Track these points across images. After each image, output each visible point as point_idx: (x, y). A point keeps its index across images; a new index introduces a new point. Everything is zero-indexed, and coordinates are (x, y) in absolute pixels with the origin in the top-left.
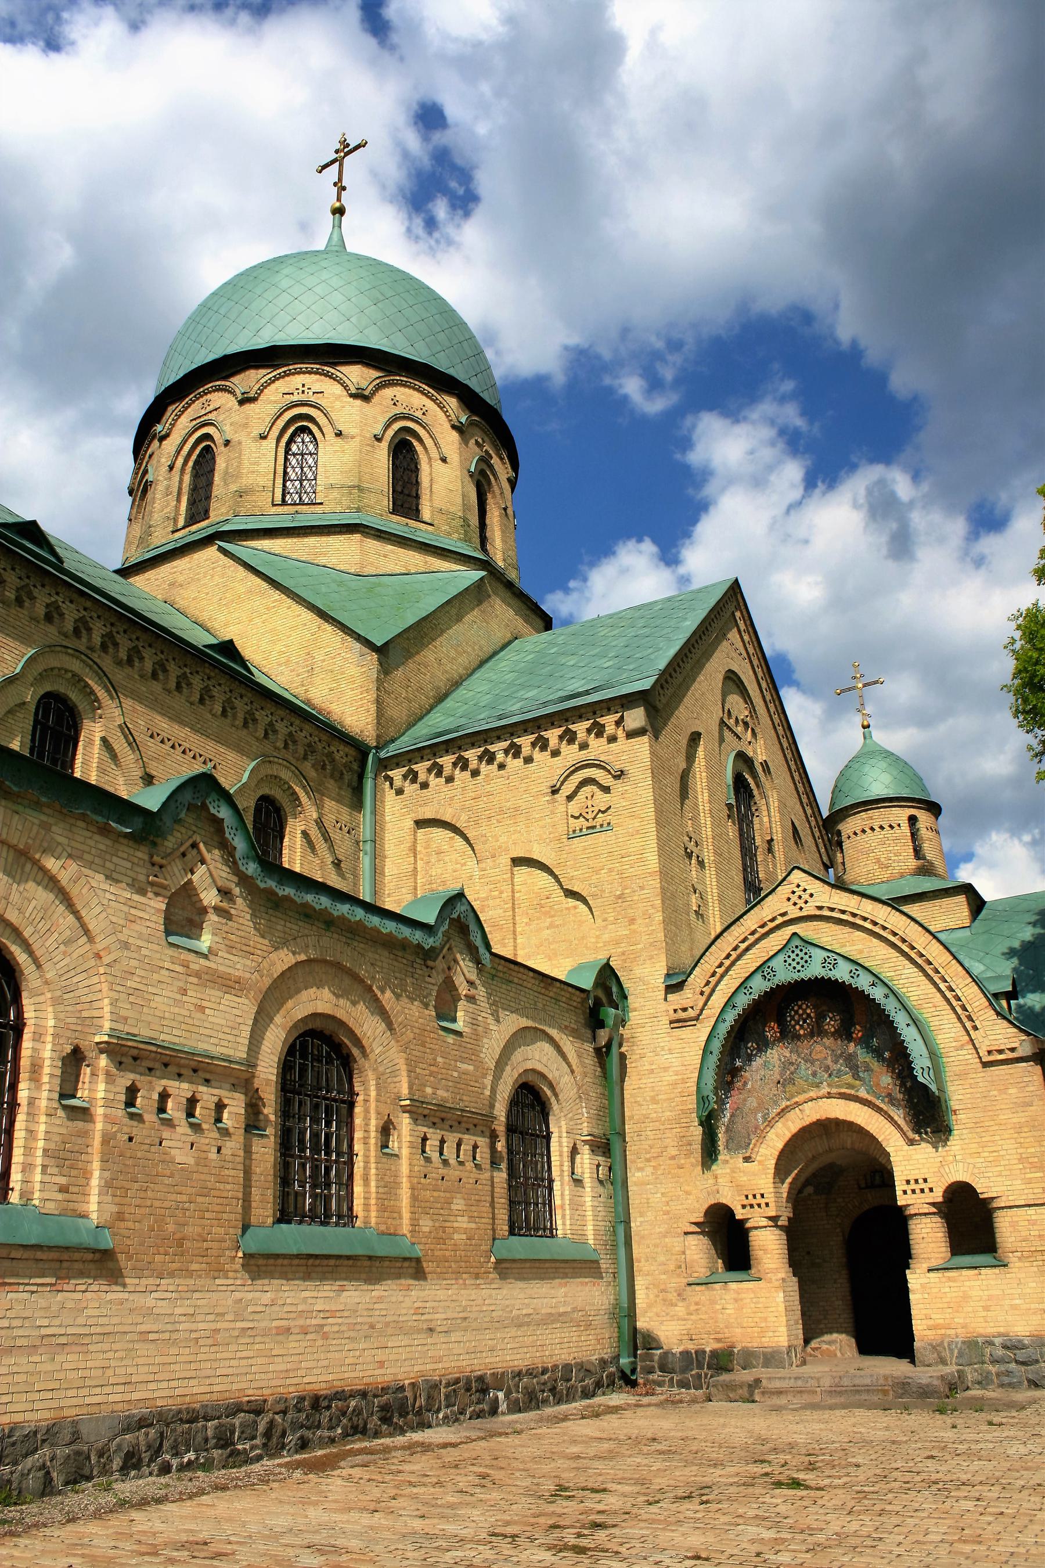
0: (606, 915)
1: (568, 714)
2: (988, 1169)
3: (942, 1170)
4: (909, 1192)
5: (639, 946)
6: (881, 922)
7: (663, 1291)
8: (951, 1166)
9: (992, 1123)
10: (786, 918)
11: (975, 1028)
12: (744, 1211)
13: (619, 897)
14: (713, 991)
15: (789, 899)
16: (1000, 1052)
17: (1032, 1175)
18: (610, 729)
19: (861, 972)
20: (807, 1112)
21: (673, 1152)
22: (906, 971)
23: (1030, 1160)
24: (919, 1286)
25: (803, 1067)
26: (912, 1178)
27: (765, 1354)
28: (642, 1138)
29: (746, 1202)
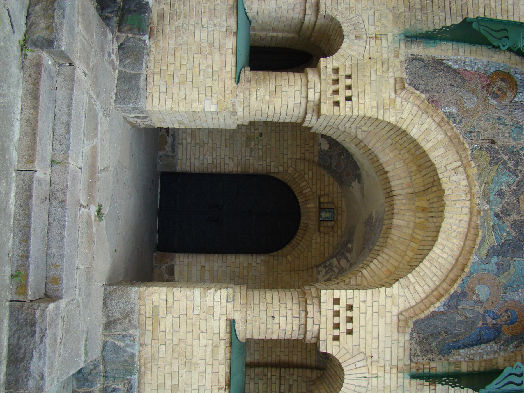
3: (361, 356)
4: (336, 308)
8: (364, 370)
12: (330, 70)
20: (454, 178)
24: (210, 304)
25: (511, 180)
26: (355, 314)
27: (137, 76)
29: (342, 73)
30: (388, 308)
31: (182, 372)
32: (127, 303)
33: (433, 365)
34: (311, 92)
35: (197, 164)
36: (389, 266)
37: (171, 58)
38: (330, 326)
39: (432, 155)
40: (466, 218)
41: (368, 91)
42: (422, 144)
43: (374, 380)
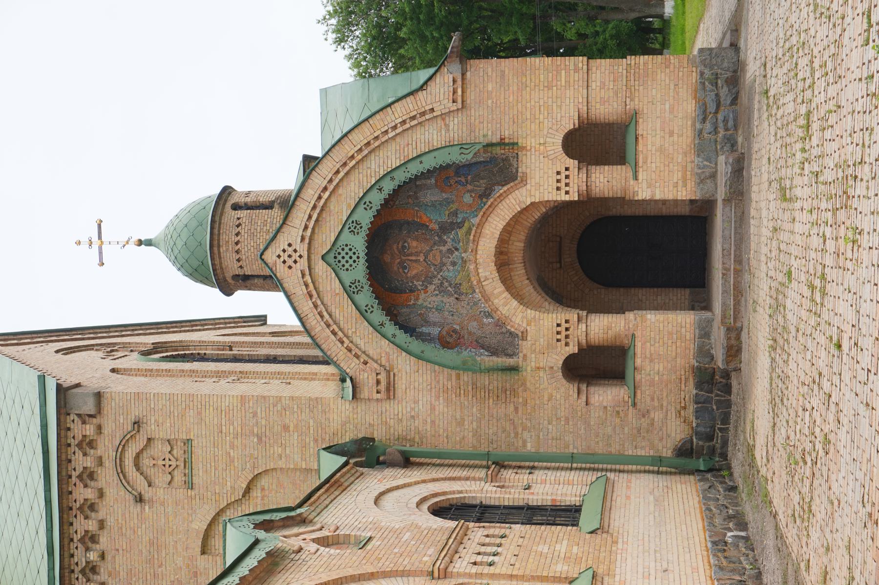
0: (276, 455)
1: (64, 457)
2: (554, 115)
3: (552, 157)
4: (567, 189)
5: (311, 424)
6: (325, 182)
7: (639, 431)
8: (549, 149)
9: (515, 108)
10: (307, 273)
11: (432, 110)
12: (571, 344)
13: (260, 439)
14: (364, 352)
15: (290, 267)
16: (455, 92)
17: (563, 79)
18: (89, 430)
19: (367, 199)
20: (488, 274)
21: (512, 408)
22: (373, 167)
23: (550, 79)
26: (555, 185)
27: (701, 337)
28: (495, 438)
29: (563, 342)
30: (533, 188)
31: (667, 145)
32: (702, 189)
33: (503, 152)
34: (584, 329)
35: (671, 294)
36: (527, 214)
37: (679, 350)
38: (571, 177)
39: (503, 288)
40: (479, 247)
41: (546, 331)
42: (509, 296)
43: (542, 142)
